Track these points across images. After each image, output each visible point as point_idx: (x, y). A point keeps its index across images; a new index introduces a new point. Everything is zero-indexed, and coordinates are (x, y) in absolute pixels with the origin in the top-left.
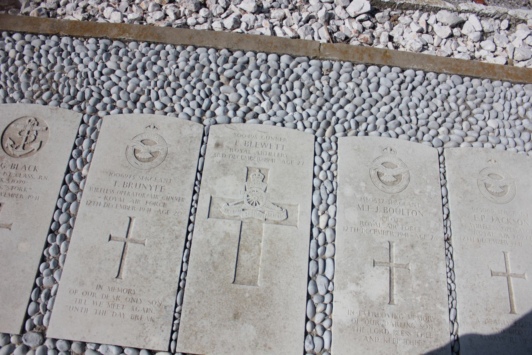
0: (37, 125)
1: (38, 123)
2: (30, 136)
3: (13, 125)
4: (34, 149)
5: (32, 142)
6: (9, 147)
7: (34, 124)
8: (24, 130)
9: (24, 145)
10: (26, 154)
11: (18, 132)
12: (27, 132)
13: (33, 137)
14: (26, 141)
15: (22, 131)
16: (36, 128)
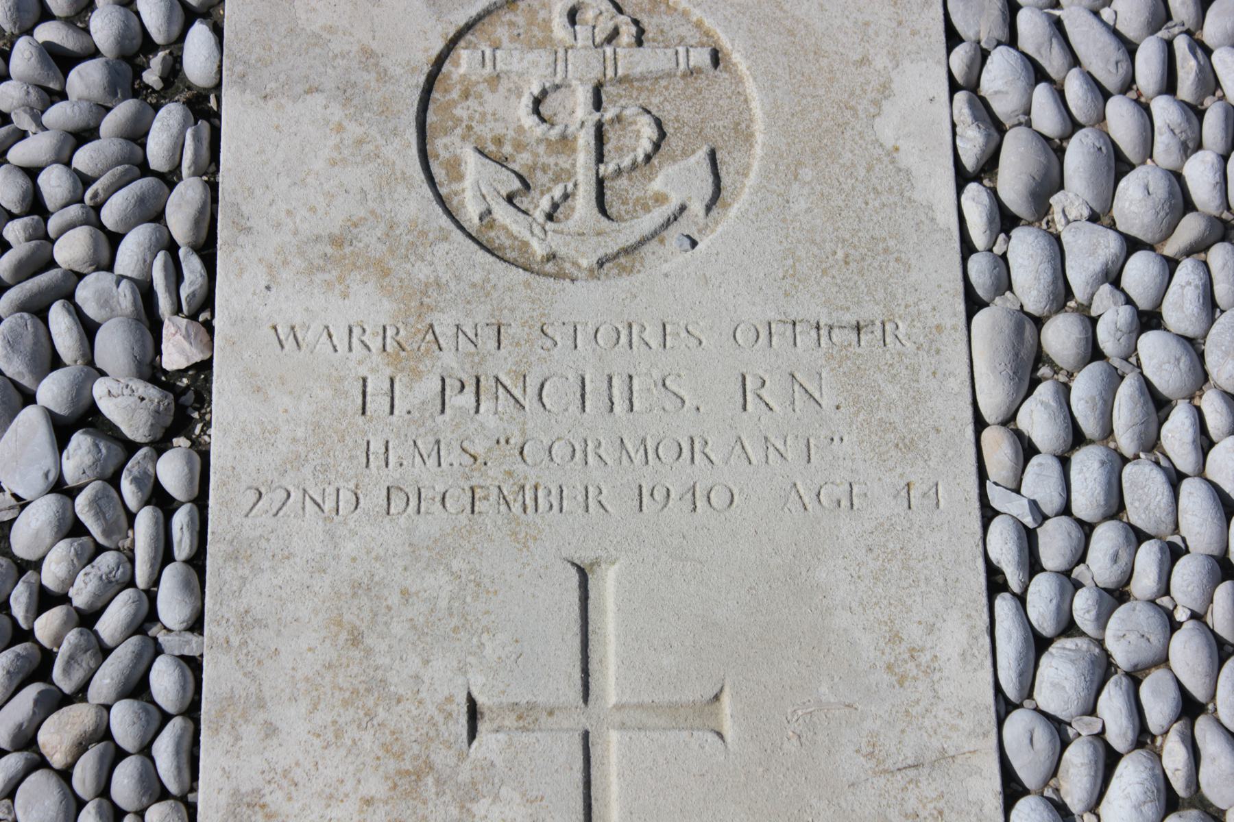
0: (639, 42)
1: (636, 22)
2: (618, 119)
3: (465, 62)
4: (683, 208)
5: (648, 158)
6: (503, 213)
7: (615, 33)
8: (557, 87)
9: (600, 183)
10: (627, 251)
11: (526, 101)
12: (582, 96)
13: (648, 132)
14: (600, 158)
15: (544, 93)
16: (631, 60)
